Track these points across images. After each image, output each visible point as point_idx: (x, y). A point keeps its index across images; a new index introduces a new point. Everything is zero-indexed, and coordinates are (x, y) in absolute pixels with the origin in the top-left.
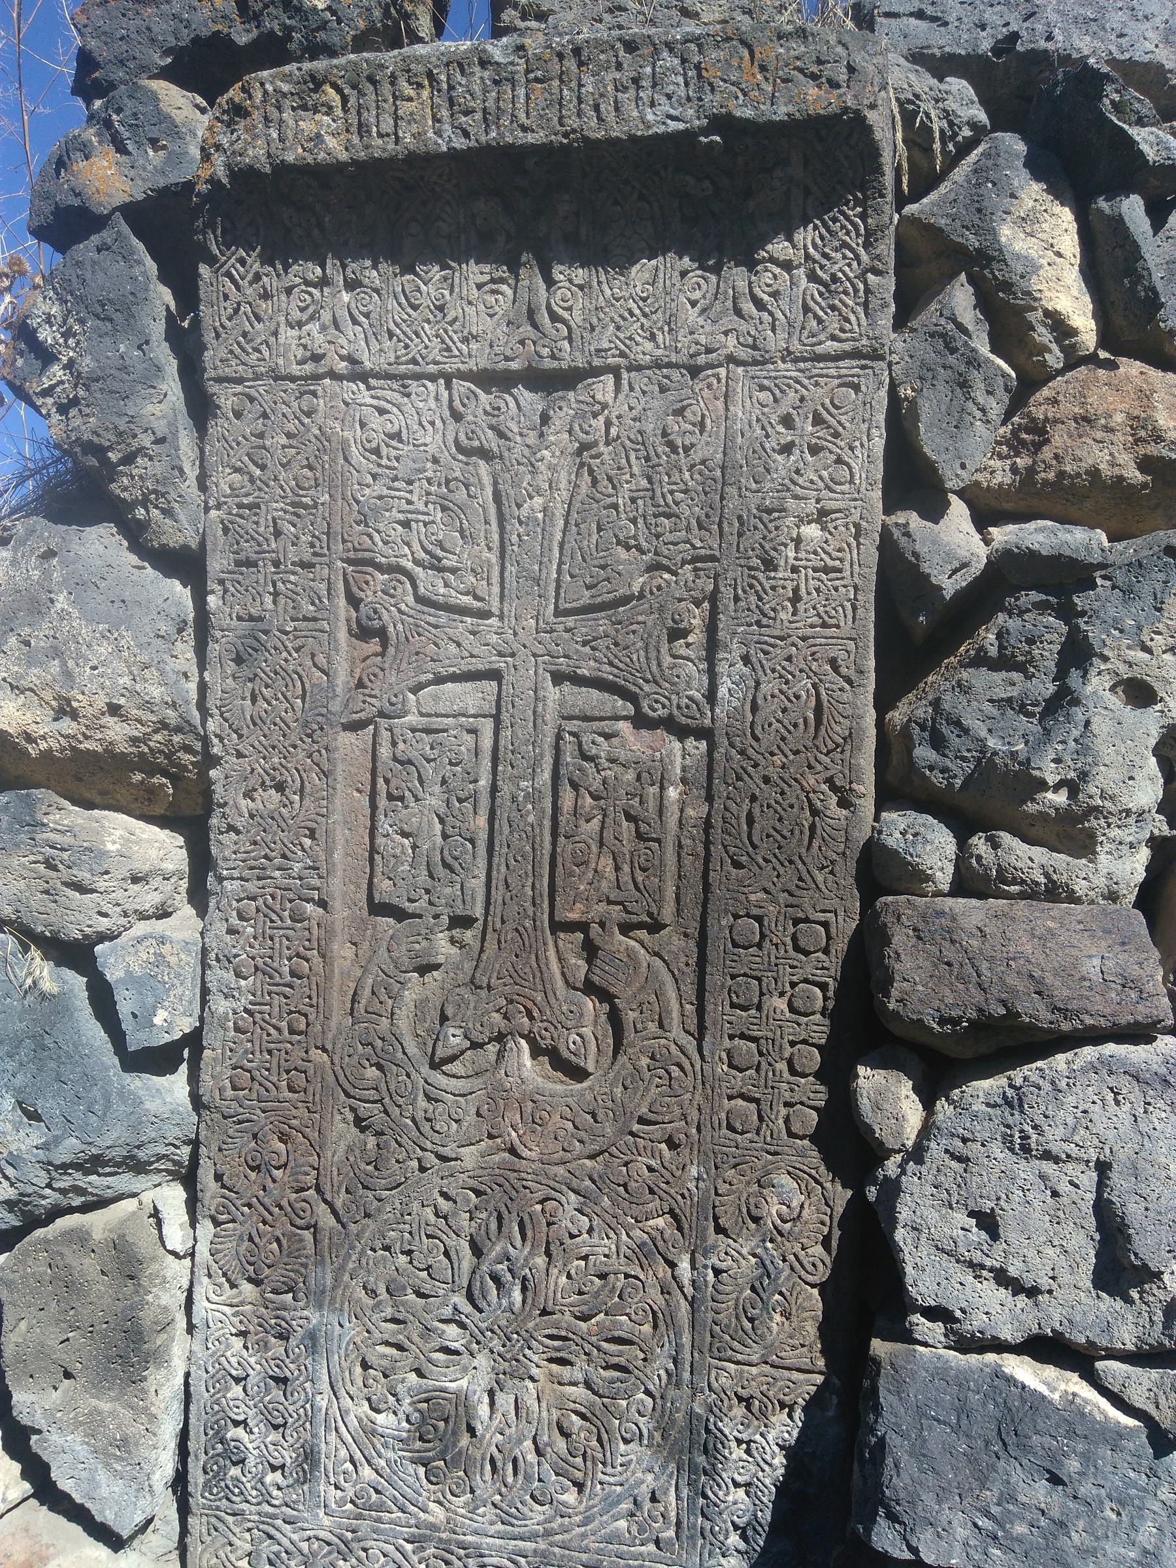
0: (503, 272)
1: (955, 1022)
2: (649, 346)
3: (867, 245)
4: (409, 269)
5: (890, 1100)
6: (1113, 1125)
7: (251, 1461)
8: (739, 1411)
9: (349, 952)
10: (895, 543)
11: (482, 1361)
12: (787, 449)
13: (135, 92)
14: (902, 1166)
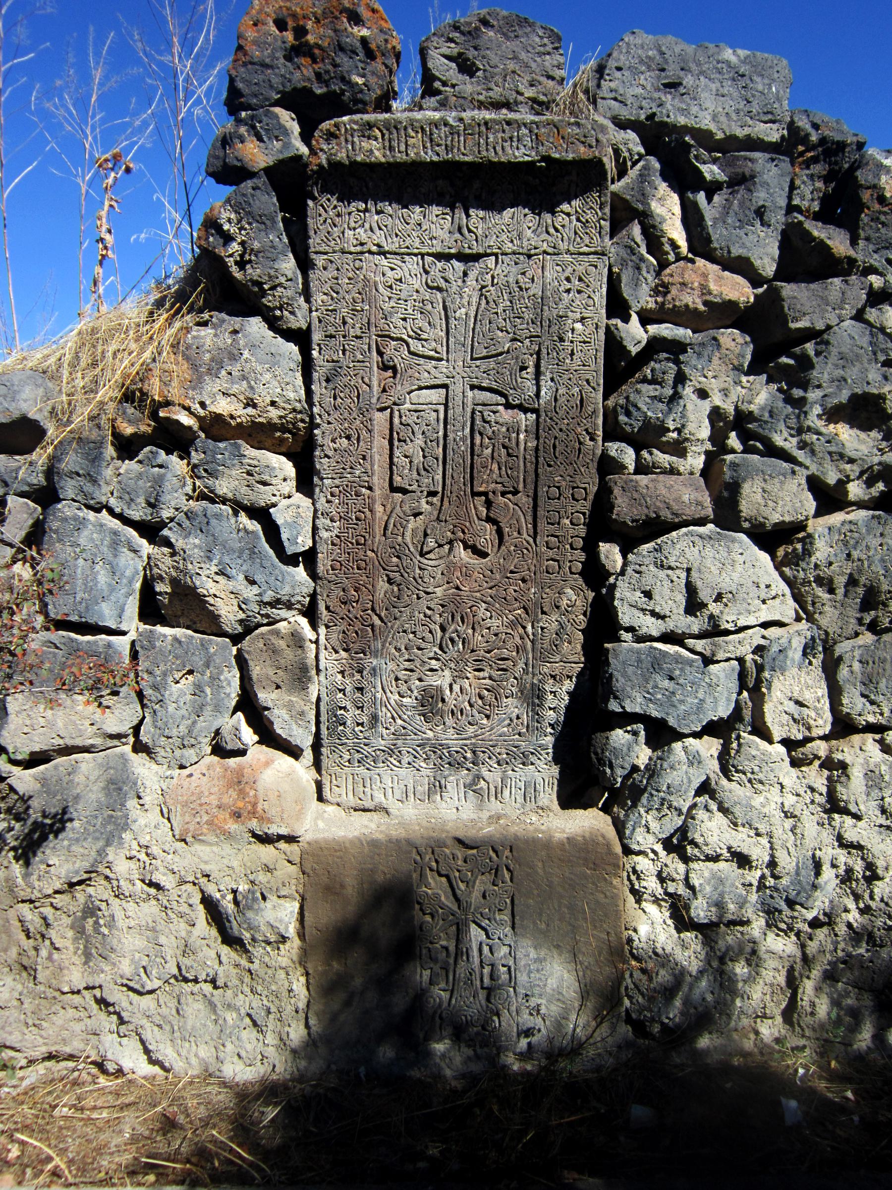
0: (448, 210)
1: (637, 521)
2: (510, 245)
3: (600, 209)
4: (405, 207)
5: (611, 554)
6: (692, 554)
7: (349, 723)
8: (551, 681)
9: (381, 509)
10: (612, 332)
11: (447, 673)
12: (568, 291)
13: (268, 114)
14: (617, 579)
